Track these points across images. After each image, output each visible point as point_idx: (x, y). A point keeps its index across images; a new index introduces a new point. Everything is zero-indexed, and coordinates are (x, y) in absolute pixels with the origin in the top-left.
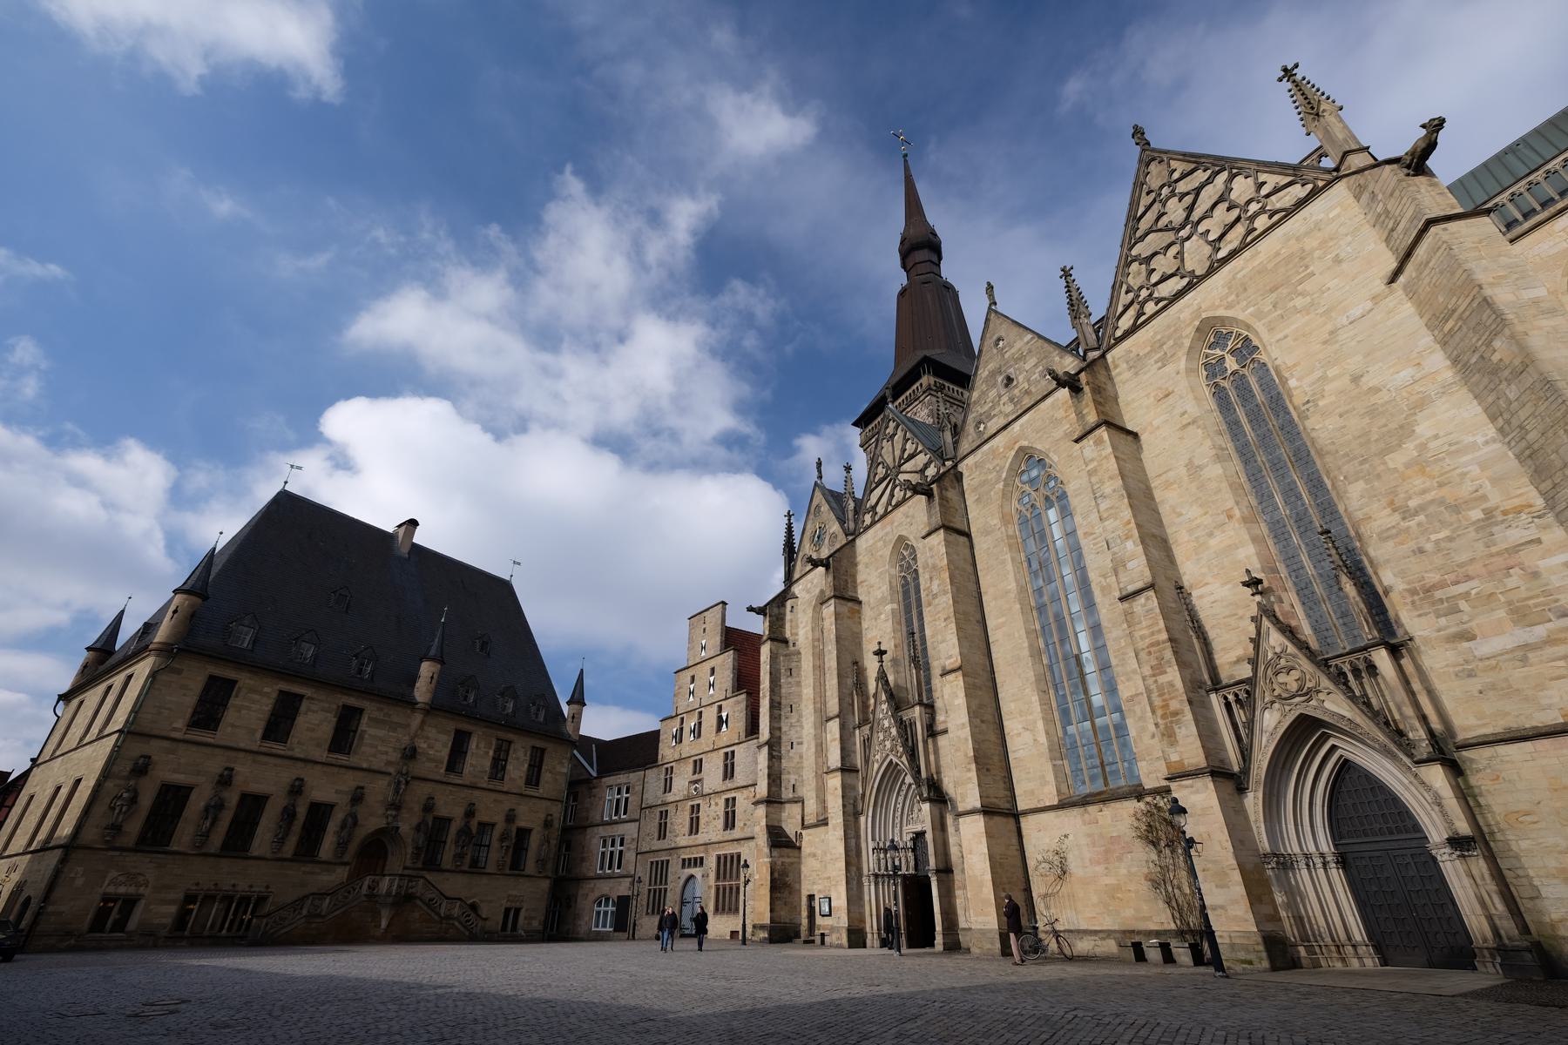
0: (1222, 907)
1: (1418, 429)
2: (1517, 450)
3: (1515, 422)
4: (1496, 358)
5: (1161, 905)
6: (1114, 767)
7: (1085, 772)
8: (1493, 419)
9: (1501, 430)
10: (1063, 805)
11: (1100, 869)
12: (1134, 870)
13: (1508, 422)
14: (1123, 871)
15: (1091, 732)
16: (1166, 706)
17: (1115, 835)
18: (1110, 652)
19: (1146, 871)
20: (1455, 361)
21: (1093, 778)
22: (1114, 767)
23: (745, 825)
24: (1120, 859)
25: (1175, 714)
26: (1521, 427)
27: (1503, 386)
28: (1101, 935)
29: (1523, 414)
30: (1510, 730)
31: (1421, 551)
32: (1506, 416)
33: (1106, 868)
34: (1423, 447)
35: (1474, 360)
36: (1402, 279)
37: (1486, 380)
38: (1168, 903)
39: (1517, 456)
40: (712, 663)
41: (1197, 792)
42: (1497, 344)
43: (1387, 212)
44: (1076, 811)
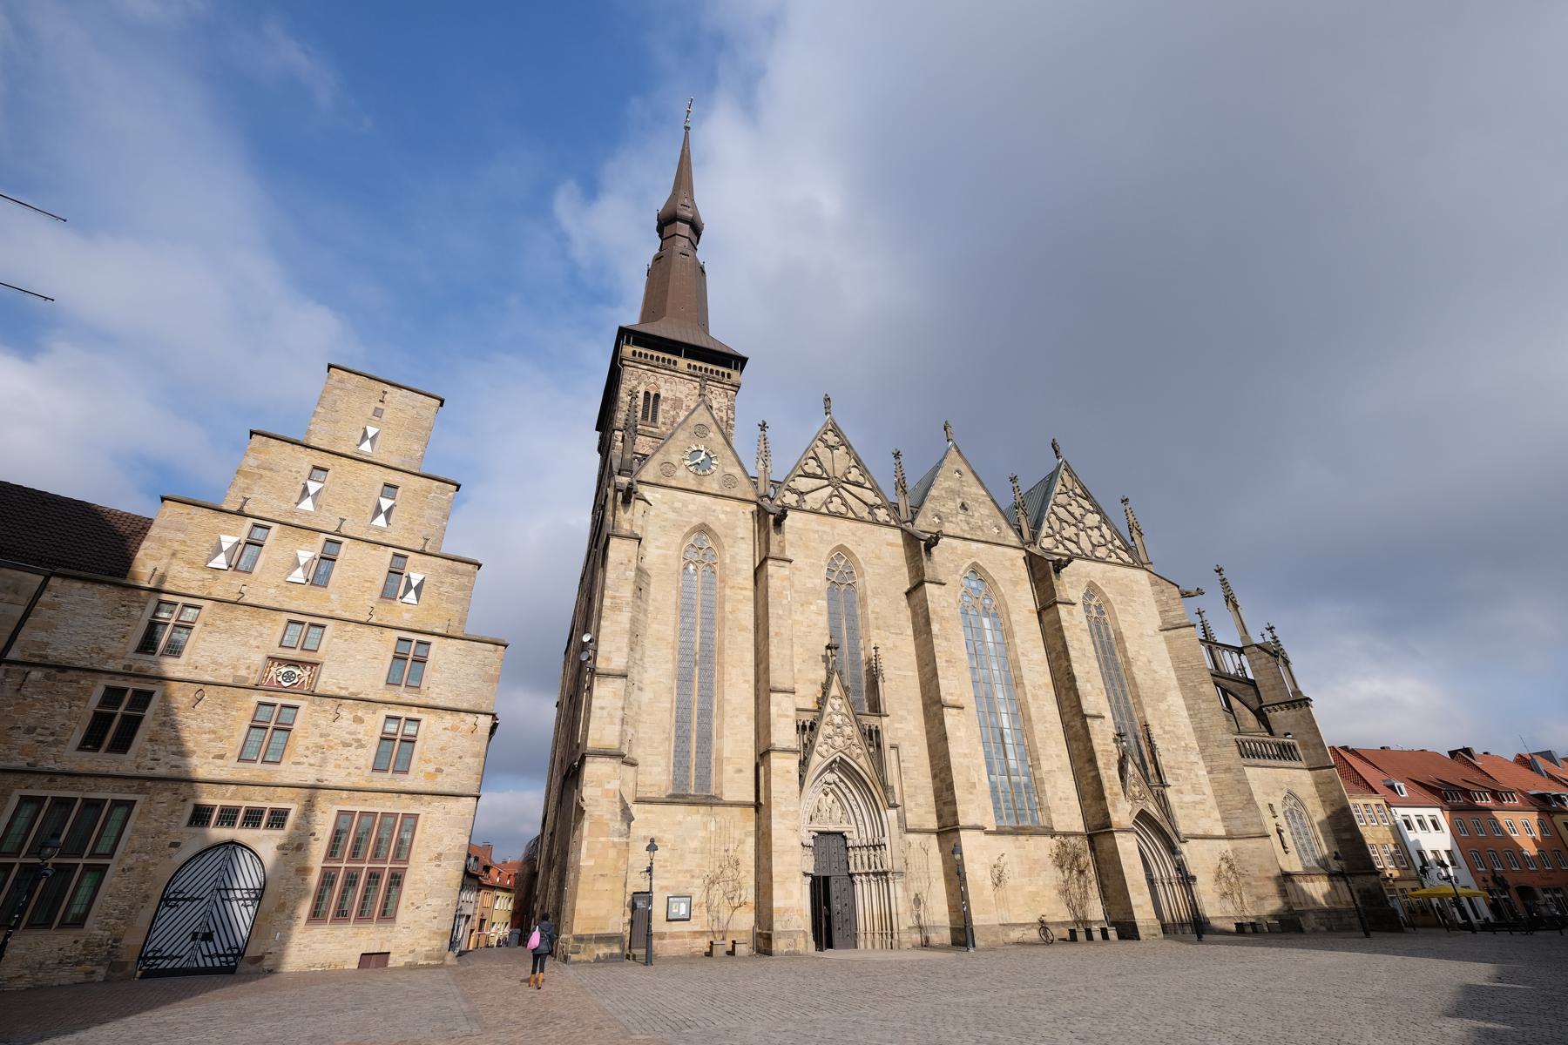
0: (1141, 906)
1: (1169, 698)
2: (1195, 726)
3: (1199, 716)
4: (1201, 690)
5: (1064, 906)
6: (1022, 812)
7: (1003, 810)
8: (1188, 709)
9: (1190, 715)
10: (1000, 832)
11: (1025, 880)
12: (1047, 882)
13: (1196, 715)
14: (1041, 883)
15: (1008, 784)
16: (1111, 789)
17: (1036, 858)
18: (1036, 738)
19: (1055, 883)
20: (1179, 679)
21: (1008, 816)
22: (1022, 812)
23: (439, 770)
24: (1039, 875)
25: (1116, 794)
27: (1200, 701)
28: (1027, 926)
29: (1204, 715)
30: (1191, 834)
31: (1168, 750)
32: (1196, 712)
33: (1030, 880)
34: (1169, 706)
37: (1192, 695)
38: (1068, 905)
39: (1194, 729)
40: (394, 478)
41: (1128, 841)
42: (1205, 686)
43: (1167, 603)
44: (1010, 838)
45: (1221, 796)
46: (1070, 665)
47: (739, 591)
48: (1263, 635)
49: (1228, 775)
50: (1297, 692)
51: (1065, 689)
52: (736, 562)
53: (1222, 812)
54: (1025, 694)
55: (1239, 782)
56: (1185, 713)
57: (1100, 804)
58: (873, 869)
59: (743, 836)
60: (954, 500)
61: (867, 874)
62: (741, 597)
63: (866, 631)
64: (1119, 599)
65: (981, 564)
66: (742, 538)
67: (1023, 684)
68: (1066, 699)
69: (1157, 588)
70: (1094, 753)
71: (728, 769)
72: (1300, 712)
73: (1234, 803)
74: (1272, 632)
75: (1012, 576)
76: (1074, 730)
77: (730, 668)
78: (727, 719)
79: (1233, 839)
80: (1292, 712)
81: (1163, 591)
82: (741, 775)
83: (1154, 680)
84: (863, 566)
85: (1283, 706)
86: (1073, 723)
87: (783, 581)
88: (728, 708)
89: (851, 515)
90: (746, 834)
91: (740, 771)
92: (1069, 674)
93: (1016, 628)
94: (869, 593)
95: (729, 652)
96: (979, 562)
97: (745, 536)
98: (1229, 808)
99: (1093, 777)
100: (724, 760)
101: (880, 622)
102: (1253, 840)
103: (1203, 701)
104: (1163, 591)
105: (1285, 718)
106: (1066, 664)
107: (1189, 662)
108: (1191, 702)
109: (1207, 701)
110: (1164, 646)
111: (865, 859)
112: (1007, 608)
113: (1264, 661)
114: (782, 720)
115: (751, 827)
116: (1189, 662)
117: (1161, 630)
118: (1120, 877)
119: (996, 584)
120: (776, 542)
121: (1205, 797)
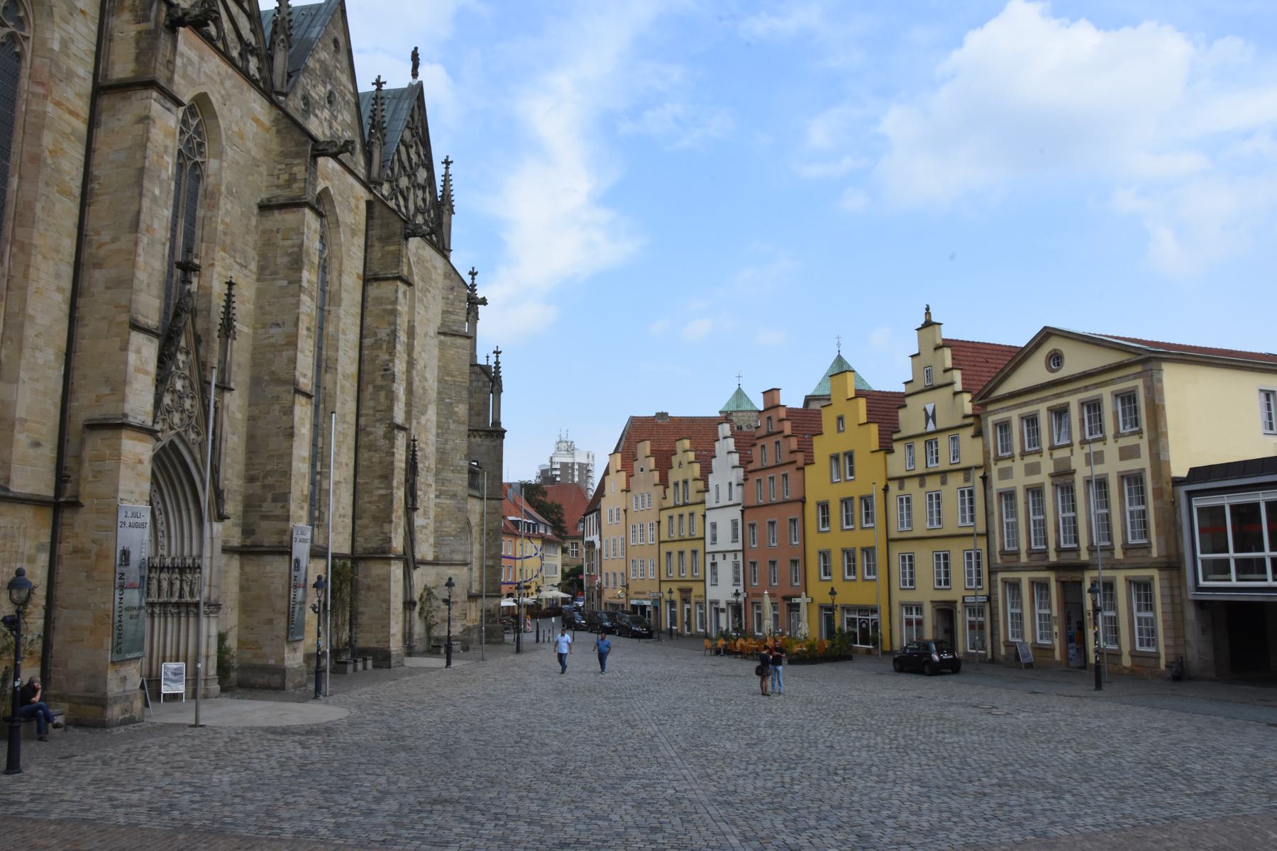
2: (439, 446)
4: (456, 409)
13: (443, 434)
20: (439, 393)
26: (446, 440)
27: (451, 421)
35: (447, 400)
36: (442, 337)
37: (445, 412)
39: (437, 449)
42: (460, 406)
43: (453, 304)
45: (440, 522)
46: (392, 361)
47: (67, 116)
48: (488, 357)
49: (453, 502)
50: (497, 423)
51: (374, 387)
52: (68, 56)
53: (436, 538)
54: (335, 383)
55: (459, 510)
56: (434, 431)
57: (382, 526)
58: (175, 599)
59: (33, 551)
60: (324, 83)
61: (165, 604)
62: (68, 130)
63: (207, 248)
64: (421, 284)
65: (332, 193)
66: (82, 12)
67: (336, 369)
68: (371, 399)
69: (448, 283)
70: (393, 470)
71: (22, 440)
72: (494, 443)
73: (449, 530)
74: (497, 357)
75: (353, 222)
76: (371, 437)
77: (39, 258)
78: (27, 352)
79: (438, 564)
80: (487, 442)
81: (452, 289)
82: (40, 451)
83: (424, 389)
84: (224, 142)
85: (481, 434)
86: (372, 429)
87: (166, 136)
88: (30, 332)
89: (220, 45)
90: (39, 548)
91: (37, 444)
92: (385, 370)
93: (344, 295)
94: (223, 189)
95: (41, 227)
96: (330, 188)
97: (87, 11)
98: (443, 534)
99: (382, 496)
100: (17, 423)
101: (228, 240)
102: (454, 567)
103: (454, 422)
104: (452, 289)
105: (479, 446)
106: (387, 357)
107: (453, 376)
108: (442, 420)
109: (458, 422)
110: (436, 352)
111: (165, 584)
112: (341, 264)
113: (481, 384)
114: (140, 376)
115: (45, 537)
116: (453, 376)
117: (439, 333)
118: (384, 605)
119: (338, 227)
120: (165, 61)
121: (428, 521)
